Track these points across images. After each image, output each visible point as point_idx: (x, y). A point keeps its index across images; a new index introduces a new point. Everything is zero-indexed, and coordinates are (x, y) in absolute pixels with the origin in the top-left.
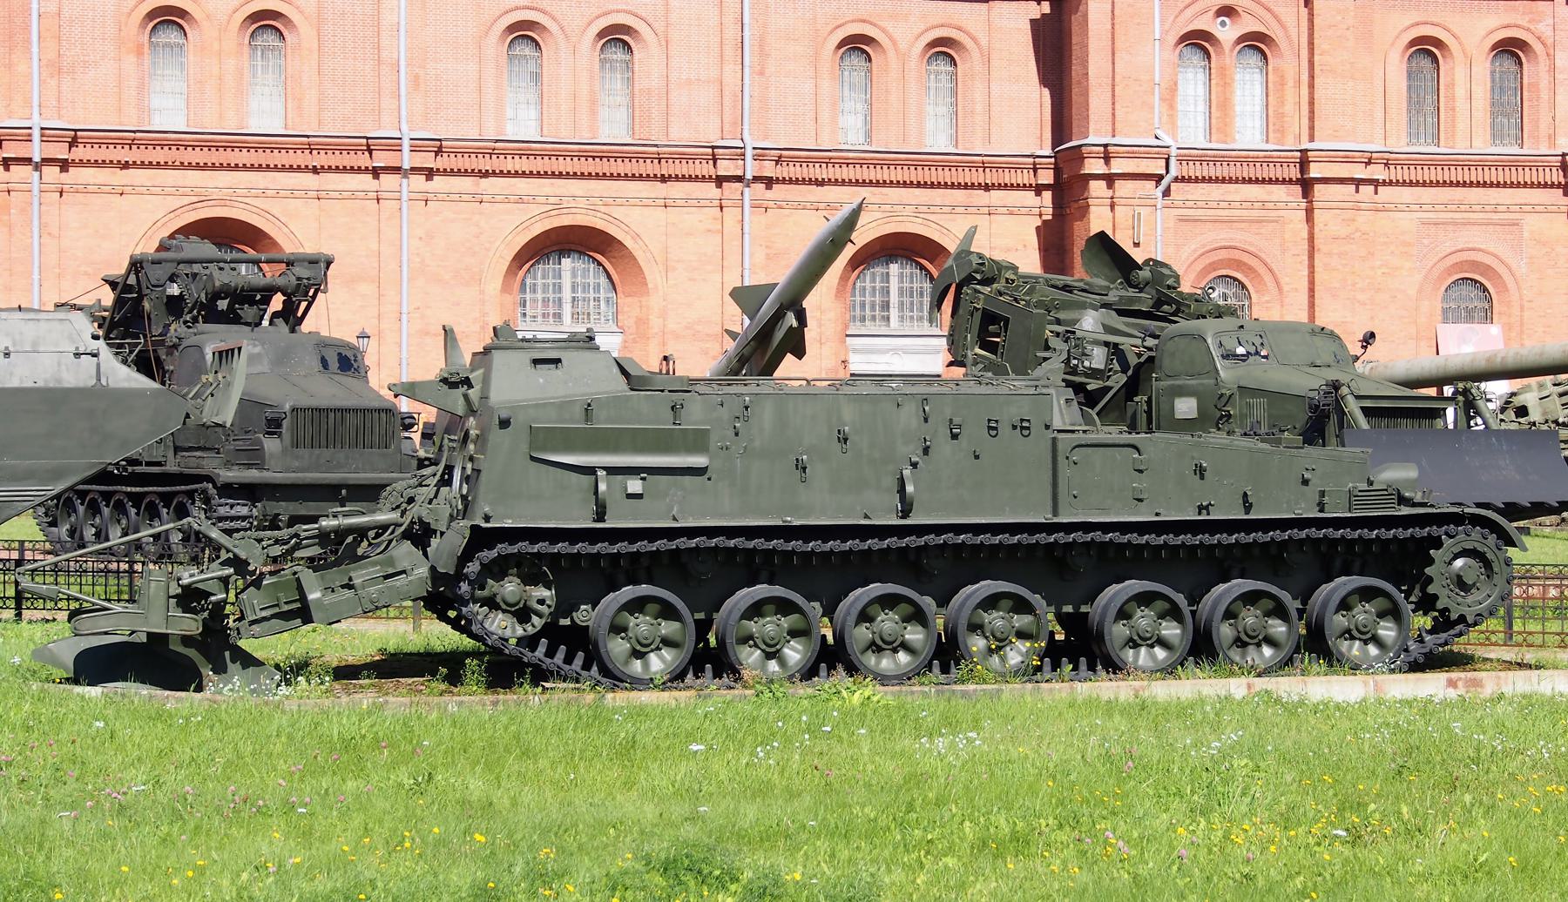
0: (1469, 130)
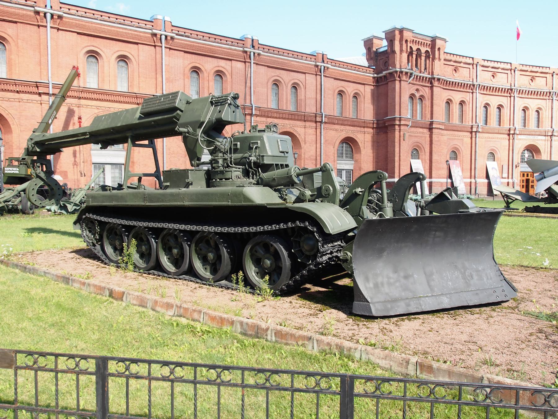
0: (456, 120)
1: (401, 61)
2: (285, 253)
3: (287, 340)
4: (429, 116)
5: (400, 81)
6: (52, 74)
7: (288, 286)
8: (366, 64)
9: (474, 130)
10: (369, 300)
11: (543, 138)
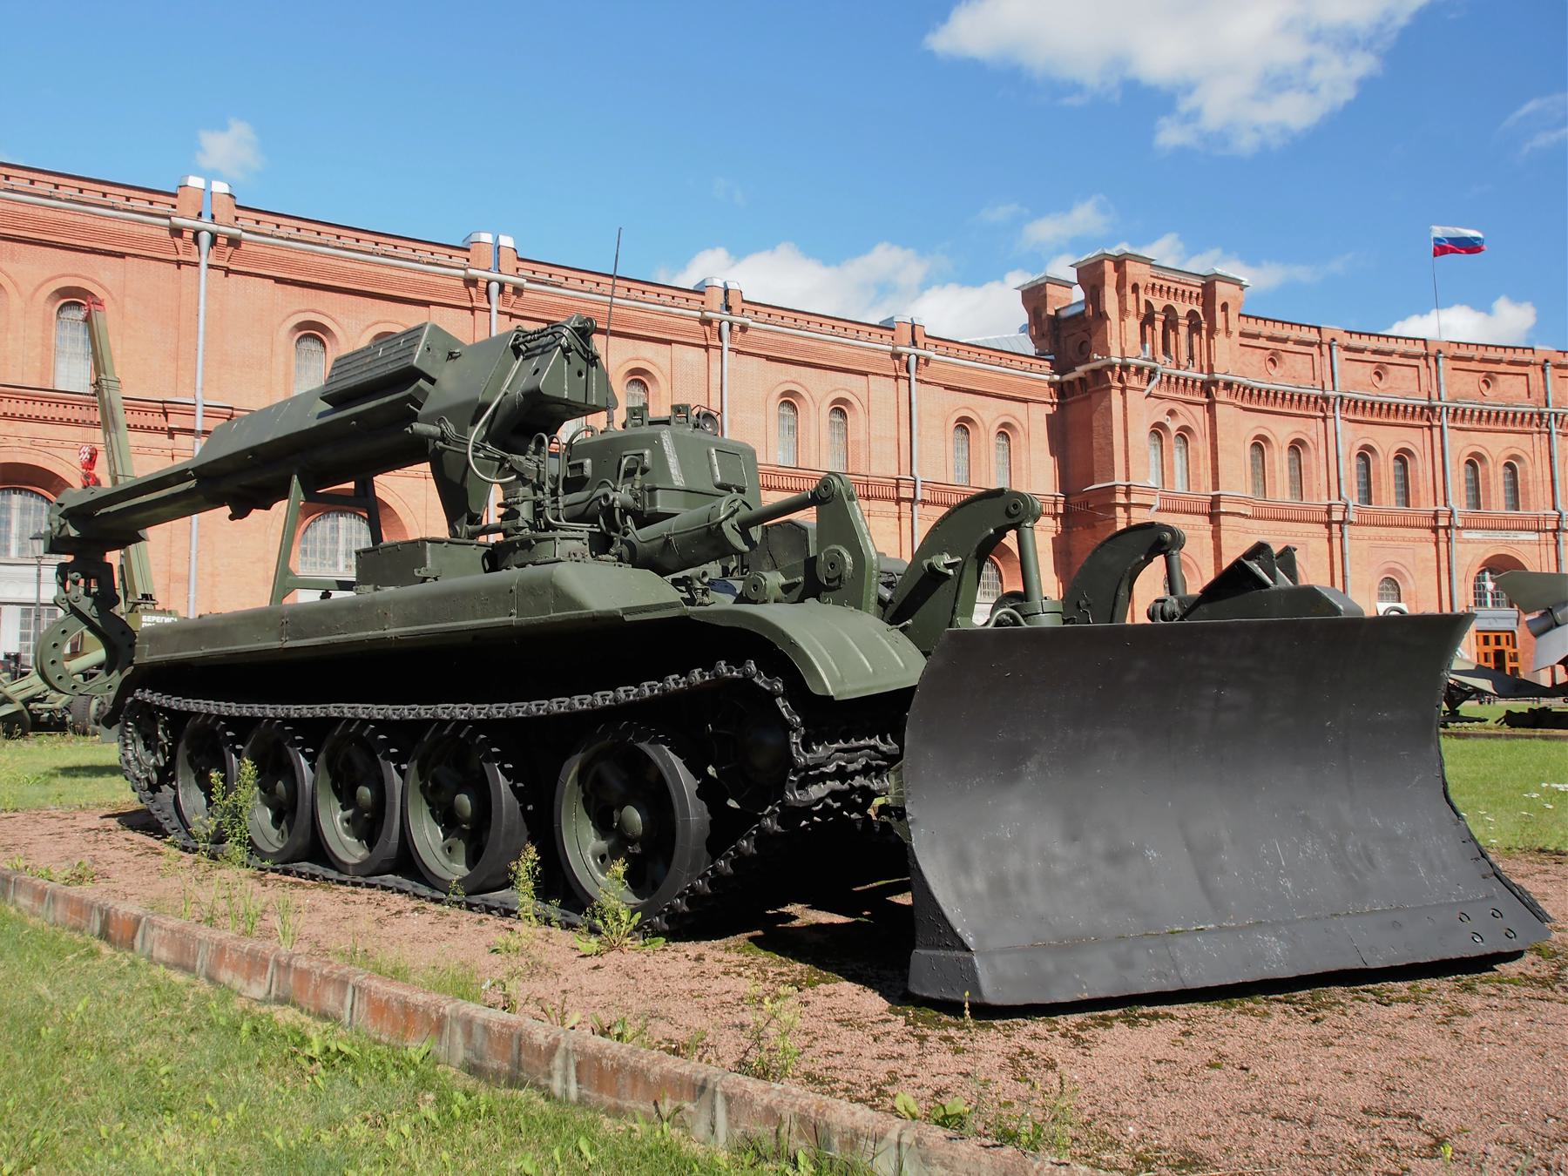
0: (1281, 490)
1: (1123, 339)
2: (687, 782)
3: (618, 1096)
4: (1207, 481)
5: (1123, 391)
6: (204, 383)
7: (694, 898)
8: (1032, 350)
9: (1337, 516)
10: (970, 940)
11: (1534, 537)
